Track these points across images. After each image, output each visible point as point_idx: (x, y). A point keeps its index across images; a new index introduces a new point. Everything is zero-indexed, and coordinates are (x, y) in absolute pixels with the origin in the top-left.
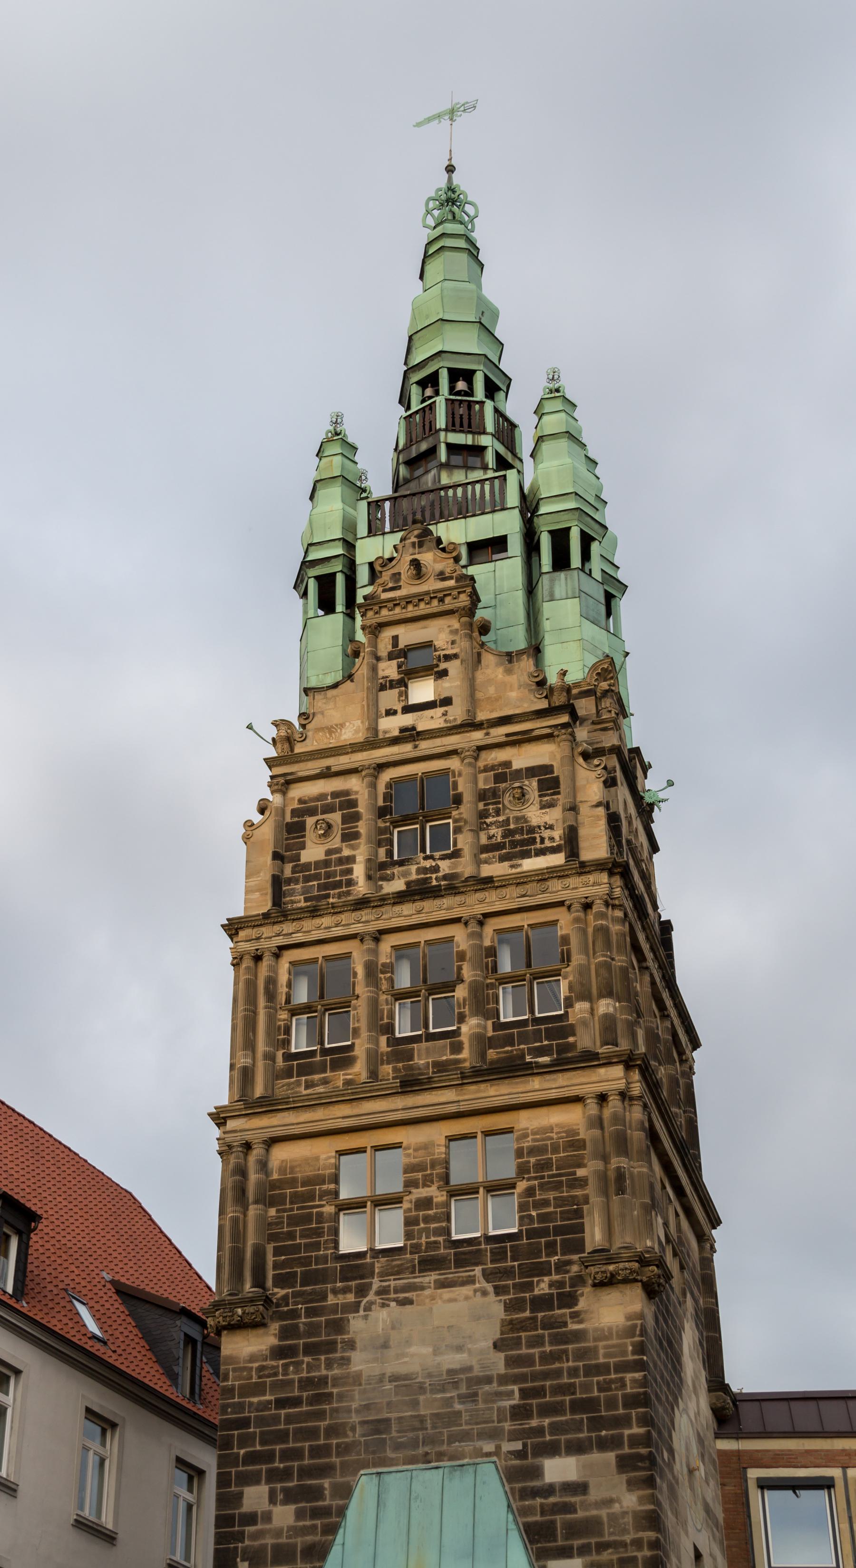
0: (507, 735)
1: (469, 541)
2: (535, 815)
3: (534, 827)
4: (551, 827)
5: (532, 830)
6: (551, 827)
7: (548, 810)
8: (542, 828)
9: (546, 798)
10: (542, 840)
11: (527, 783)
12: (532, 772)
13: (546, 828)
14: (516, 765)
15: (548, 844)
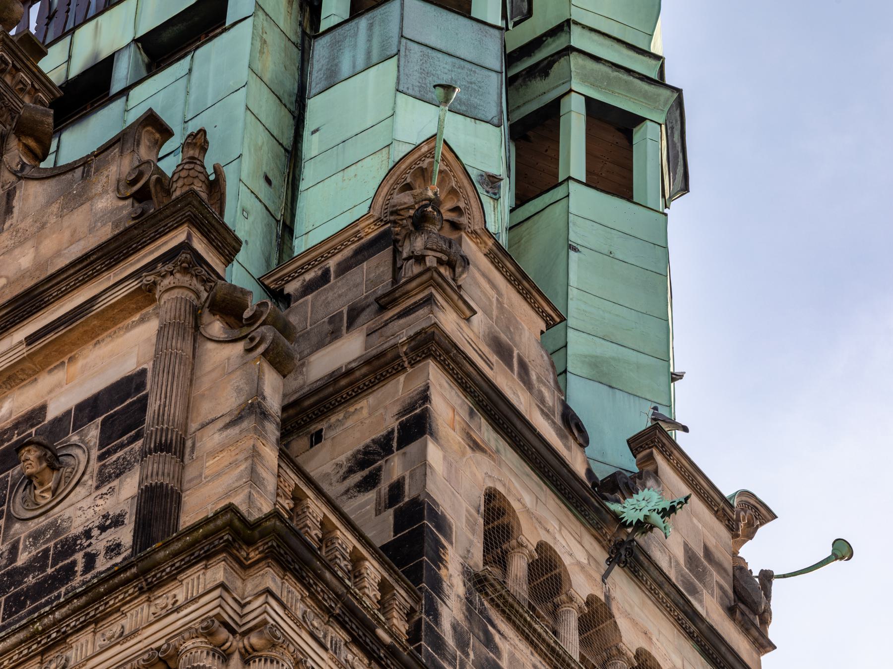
0: (30, 340)
1: (141, 32)
2: (81, 509)
3: (76, 538)
4: (118, 521)
5: (68, 547)
6: (118, 521)
7: (115, 483)
8: (95, 532)
9: (114, 457)
10: (90, 560)
11: (75, 438)
12: (88, 409)
13: (103, 528)
14: (52, 414)
15: (102, 565)
